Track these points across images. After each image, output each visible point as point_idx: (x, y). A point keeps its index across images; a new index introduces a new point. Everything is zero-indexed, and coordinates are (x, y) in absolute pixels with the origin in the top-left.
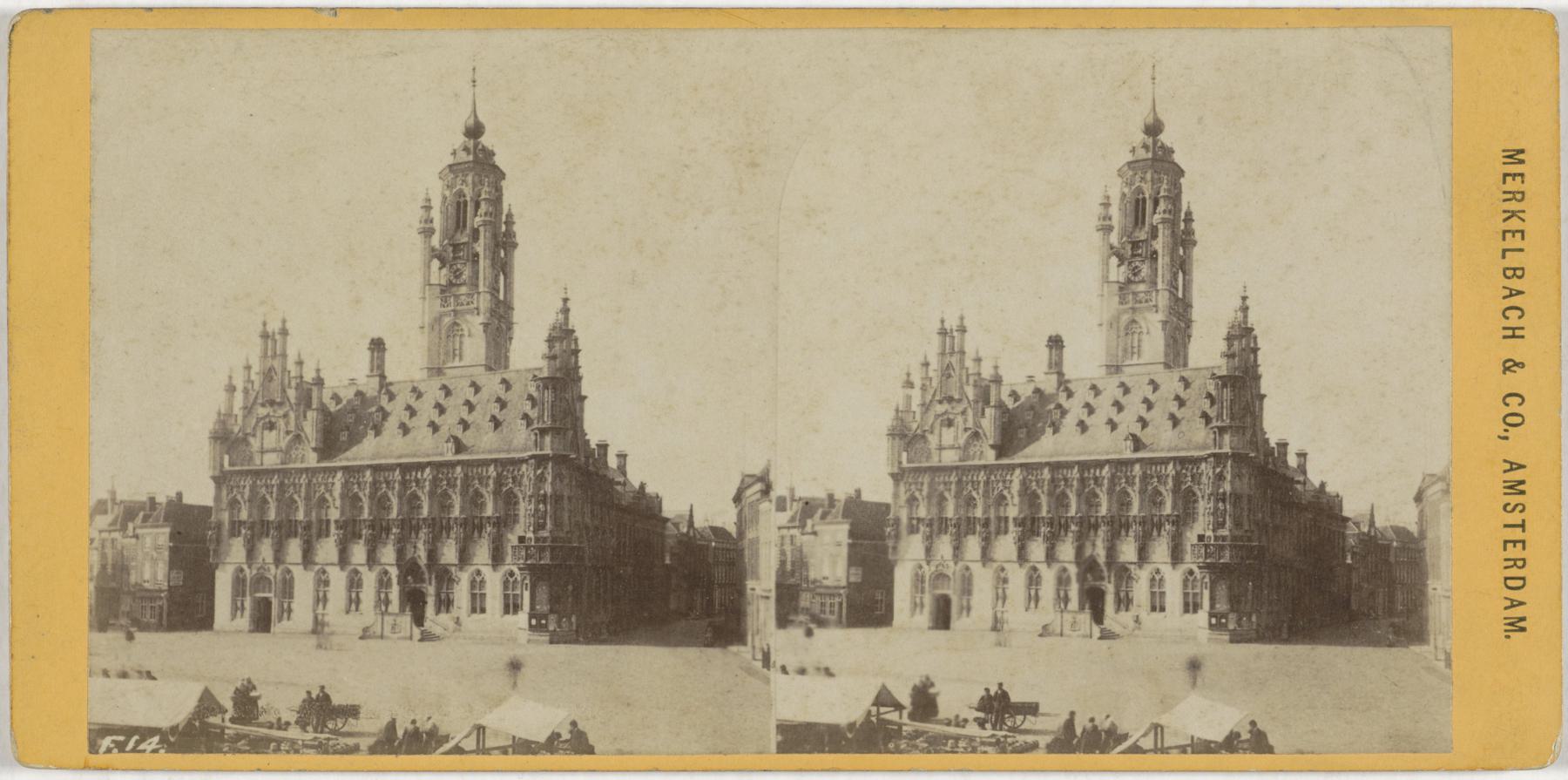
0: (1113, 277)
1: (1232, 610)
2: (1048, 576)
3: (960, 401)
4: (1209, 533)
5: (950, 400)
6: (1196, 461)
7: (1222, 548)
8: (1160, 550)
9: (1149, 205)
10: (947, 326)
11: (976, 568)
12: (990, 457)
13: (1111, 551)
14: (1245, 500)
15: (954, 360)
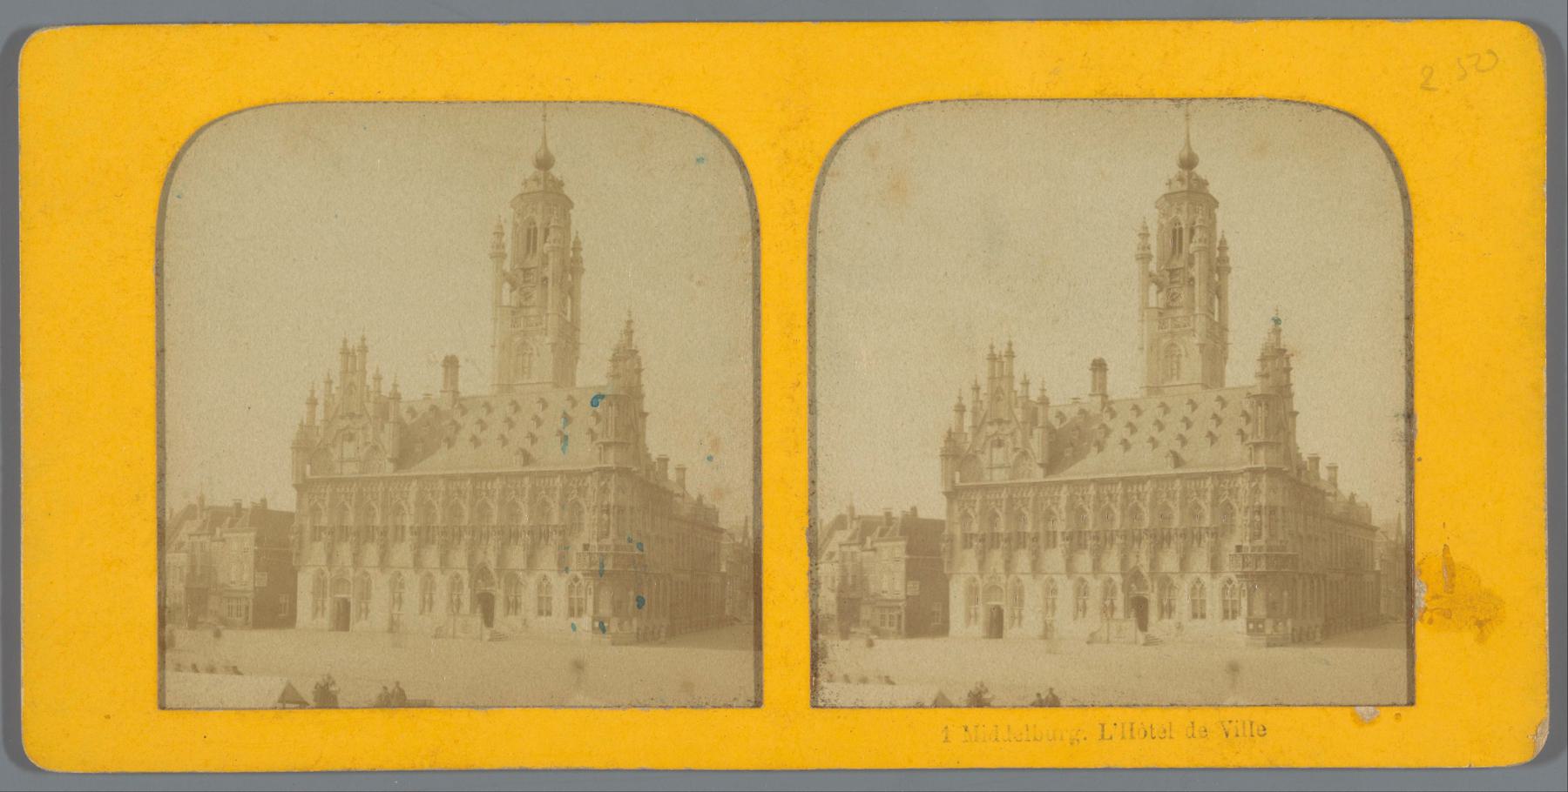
0: (1153, 303)
1: (1268, 616)
2: (1095, 585)
3: (1009, 422)
4: (1246, 544)
5: (1000, 422)
6: (1233, 476)
7: (1258, 558)
8: (1200, 561)
10: (996, 352)
11: (1027, 580)
12: (1039, 475)
14: (1280, 512)
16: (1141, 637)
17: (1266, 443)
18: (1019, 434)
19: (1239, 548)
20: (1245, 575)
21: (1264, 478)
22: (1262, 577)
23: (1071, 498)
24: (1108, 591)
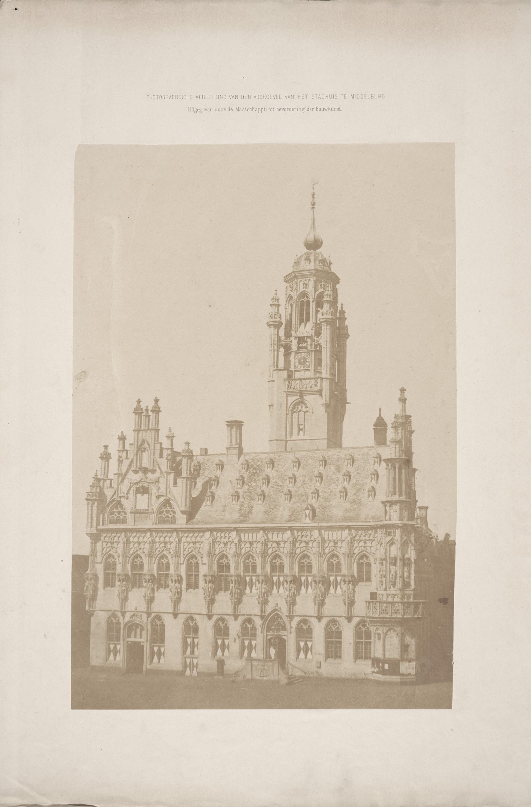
3: (153, 471)
5: (145, 470)
9: (313, 306)
10: (143, 406)
15: (149, 436)
18: (162, 480)
19: (373, 596)
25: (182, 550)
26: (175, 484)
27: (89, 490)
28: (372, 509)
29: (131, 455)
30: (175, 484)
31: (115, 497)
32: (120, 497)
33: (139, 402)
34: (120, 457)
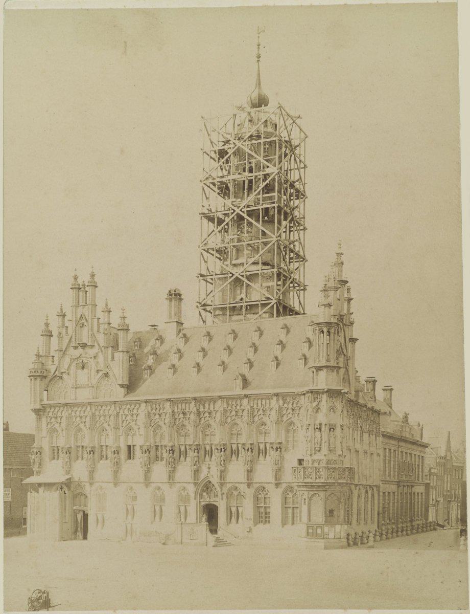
2: (171, 495)
3: (92, 346)
4: (307, 458)
5: (84, 346)
6: (295, 396)
13: (223, 474)
14: (338, 429)
15: (87, 311)
16: (211, 538)
17: (327, 367)
20: (306, 485)
21: (325, 397)
22: (324, 486)
23: (149, 415)
24: (185, 499)
25: (120, 422)
26: (113, 358)
27: (31, 366)
28: (299, 377)
29: (70, 331)
30: (113, 358)
31: (57, 373)
32: (62, 373)
33: (76, 278)
34: (60, 333)
